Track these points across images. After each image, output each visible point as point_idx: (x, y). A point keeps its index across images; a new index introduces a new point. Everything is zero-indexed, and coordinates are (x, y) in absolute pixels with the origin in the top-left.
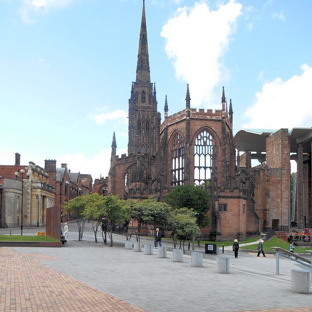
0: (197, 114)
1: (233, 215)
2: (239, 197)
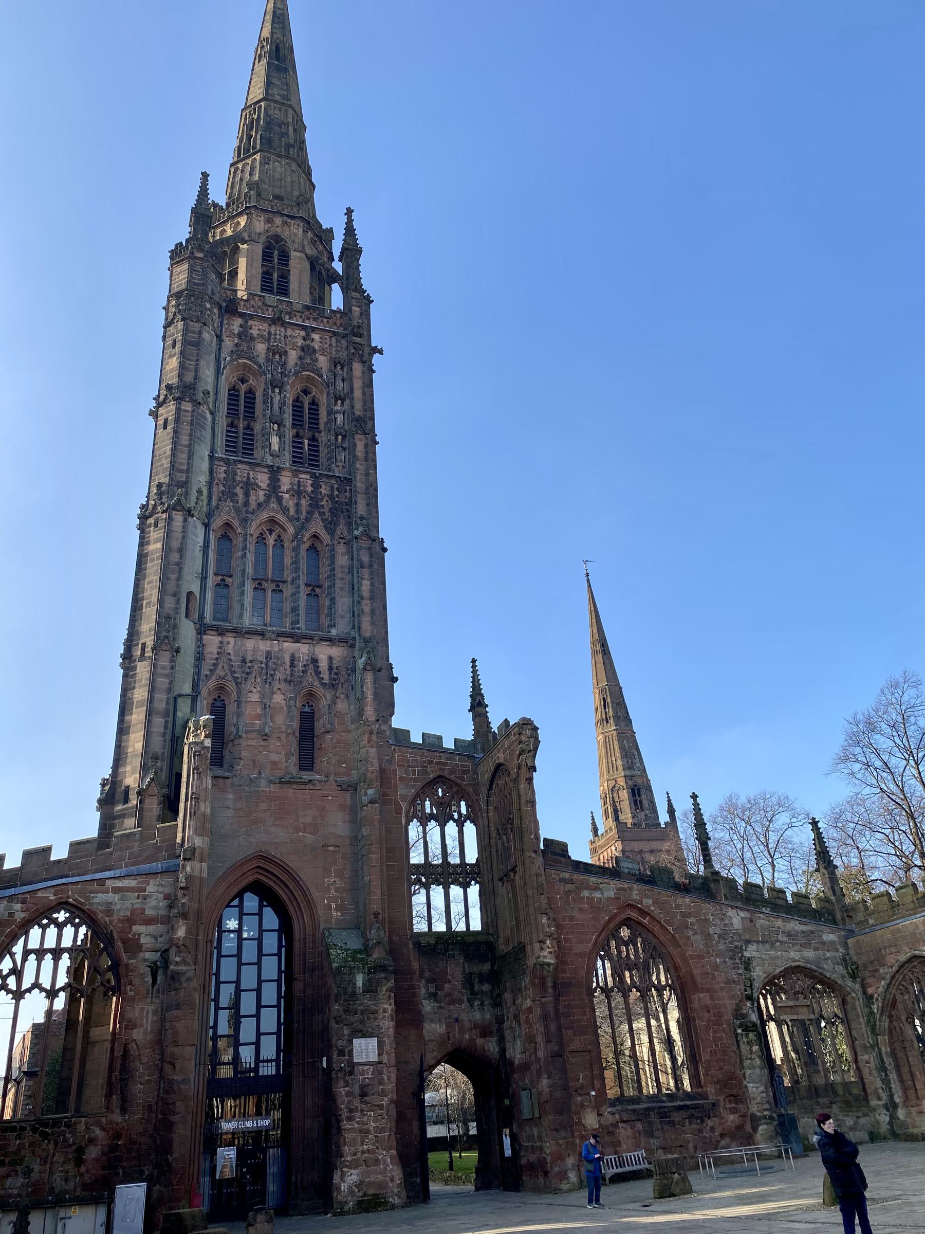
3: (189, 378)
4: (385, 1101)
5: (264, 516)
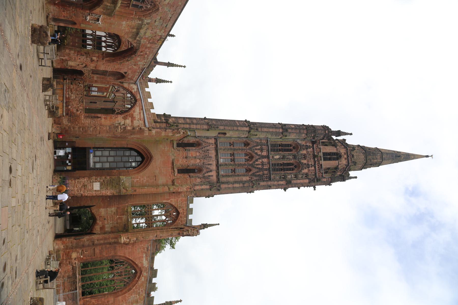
3: (289, 130)
4: (82, 192)
5: (254, 154)
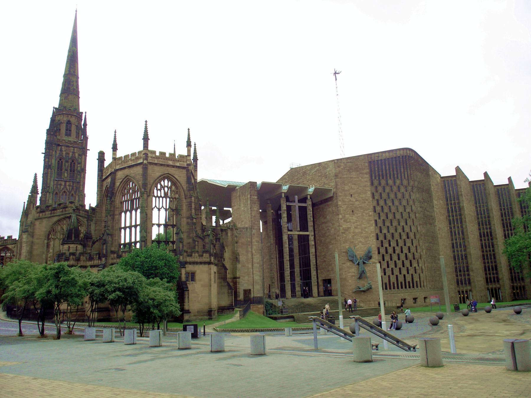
0: (157, 157)
1: (203, 286)
2: (209, 263)
3: (50, 164)
5: (63, 191)
